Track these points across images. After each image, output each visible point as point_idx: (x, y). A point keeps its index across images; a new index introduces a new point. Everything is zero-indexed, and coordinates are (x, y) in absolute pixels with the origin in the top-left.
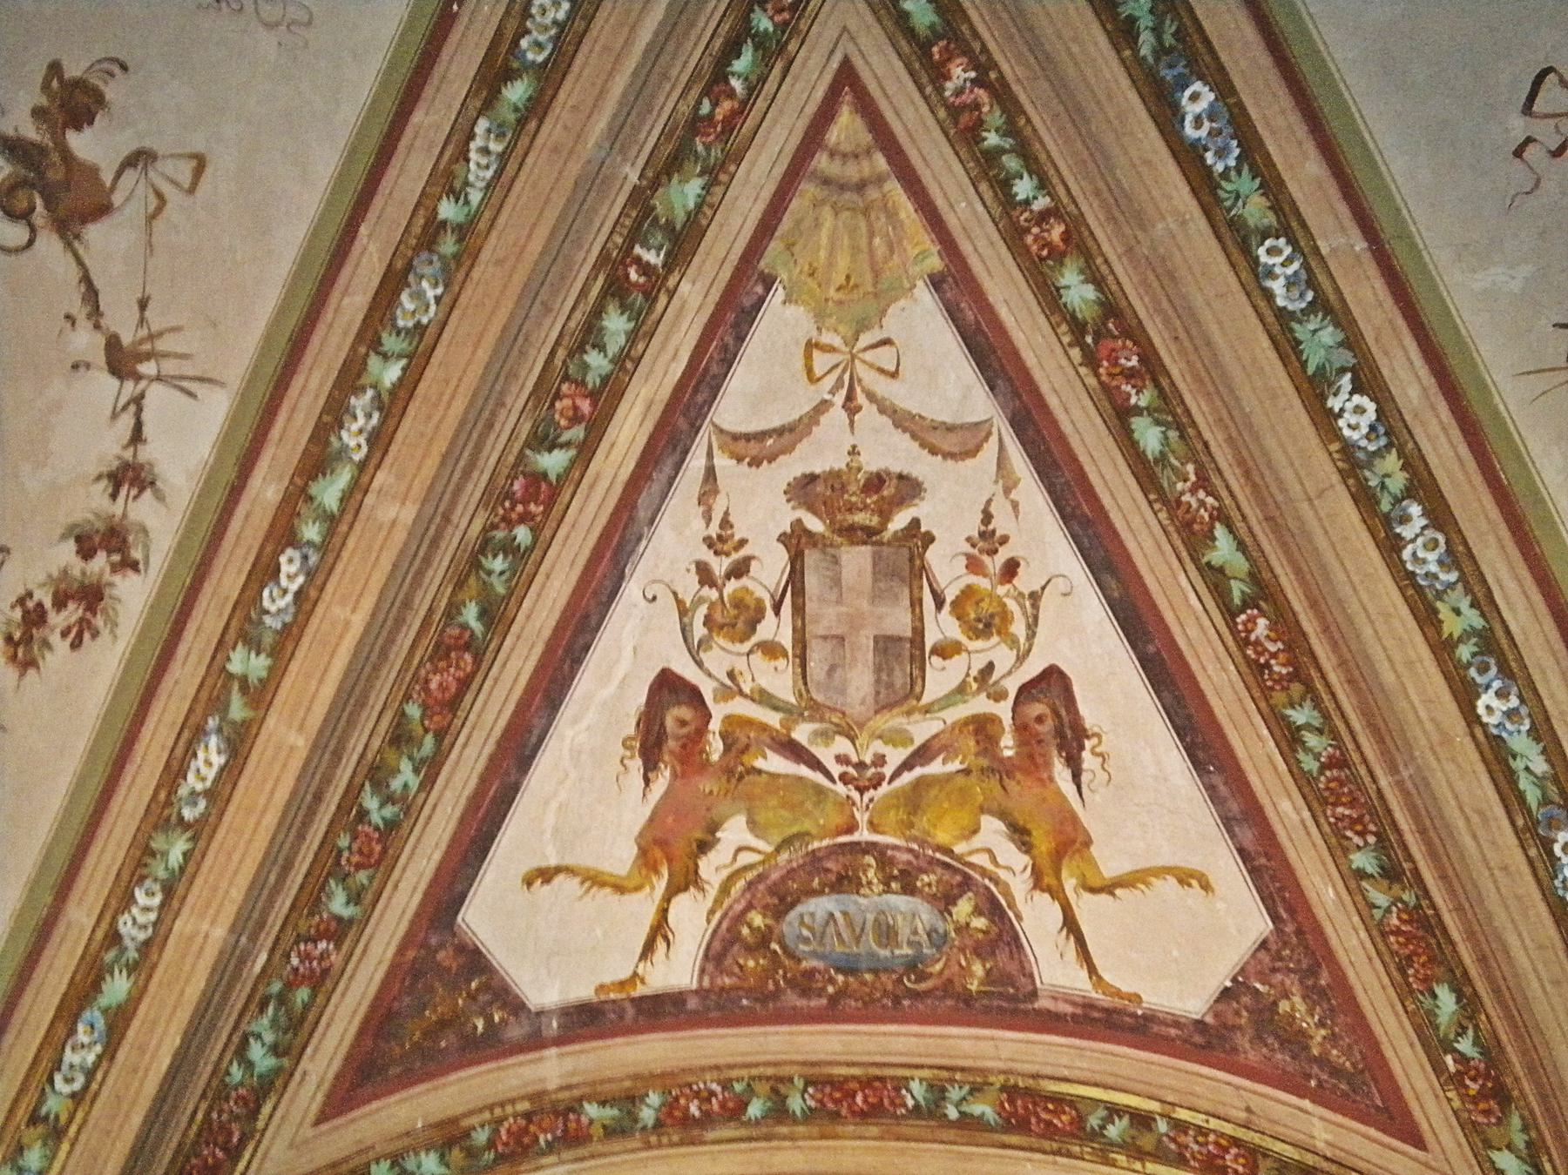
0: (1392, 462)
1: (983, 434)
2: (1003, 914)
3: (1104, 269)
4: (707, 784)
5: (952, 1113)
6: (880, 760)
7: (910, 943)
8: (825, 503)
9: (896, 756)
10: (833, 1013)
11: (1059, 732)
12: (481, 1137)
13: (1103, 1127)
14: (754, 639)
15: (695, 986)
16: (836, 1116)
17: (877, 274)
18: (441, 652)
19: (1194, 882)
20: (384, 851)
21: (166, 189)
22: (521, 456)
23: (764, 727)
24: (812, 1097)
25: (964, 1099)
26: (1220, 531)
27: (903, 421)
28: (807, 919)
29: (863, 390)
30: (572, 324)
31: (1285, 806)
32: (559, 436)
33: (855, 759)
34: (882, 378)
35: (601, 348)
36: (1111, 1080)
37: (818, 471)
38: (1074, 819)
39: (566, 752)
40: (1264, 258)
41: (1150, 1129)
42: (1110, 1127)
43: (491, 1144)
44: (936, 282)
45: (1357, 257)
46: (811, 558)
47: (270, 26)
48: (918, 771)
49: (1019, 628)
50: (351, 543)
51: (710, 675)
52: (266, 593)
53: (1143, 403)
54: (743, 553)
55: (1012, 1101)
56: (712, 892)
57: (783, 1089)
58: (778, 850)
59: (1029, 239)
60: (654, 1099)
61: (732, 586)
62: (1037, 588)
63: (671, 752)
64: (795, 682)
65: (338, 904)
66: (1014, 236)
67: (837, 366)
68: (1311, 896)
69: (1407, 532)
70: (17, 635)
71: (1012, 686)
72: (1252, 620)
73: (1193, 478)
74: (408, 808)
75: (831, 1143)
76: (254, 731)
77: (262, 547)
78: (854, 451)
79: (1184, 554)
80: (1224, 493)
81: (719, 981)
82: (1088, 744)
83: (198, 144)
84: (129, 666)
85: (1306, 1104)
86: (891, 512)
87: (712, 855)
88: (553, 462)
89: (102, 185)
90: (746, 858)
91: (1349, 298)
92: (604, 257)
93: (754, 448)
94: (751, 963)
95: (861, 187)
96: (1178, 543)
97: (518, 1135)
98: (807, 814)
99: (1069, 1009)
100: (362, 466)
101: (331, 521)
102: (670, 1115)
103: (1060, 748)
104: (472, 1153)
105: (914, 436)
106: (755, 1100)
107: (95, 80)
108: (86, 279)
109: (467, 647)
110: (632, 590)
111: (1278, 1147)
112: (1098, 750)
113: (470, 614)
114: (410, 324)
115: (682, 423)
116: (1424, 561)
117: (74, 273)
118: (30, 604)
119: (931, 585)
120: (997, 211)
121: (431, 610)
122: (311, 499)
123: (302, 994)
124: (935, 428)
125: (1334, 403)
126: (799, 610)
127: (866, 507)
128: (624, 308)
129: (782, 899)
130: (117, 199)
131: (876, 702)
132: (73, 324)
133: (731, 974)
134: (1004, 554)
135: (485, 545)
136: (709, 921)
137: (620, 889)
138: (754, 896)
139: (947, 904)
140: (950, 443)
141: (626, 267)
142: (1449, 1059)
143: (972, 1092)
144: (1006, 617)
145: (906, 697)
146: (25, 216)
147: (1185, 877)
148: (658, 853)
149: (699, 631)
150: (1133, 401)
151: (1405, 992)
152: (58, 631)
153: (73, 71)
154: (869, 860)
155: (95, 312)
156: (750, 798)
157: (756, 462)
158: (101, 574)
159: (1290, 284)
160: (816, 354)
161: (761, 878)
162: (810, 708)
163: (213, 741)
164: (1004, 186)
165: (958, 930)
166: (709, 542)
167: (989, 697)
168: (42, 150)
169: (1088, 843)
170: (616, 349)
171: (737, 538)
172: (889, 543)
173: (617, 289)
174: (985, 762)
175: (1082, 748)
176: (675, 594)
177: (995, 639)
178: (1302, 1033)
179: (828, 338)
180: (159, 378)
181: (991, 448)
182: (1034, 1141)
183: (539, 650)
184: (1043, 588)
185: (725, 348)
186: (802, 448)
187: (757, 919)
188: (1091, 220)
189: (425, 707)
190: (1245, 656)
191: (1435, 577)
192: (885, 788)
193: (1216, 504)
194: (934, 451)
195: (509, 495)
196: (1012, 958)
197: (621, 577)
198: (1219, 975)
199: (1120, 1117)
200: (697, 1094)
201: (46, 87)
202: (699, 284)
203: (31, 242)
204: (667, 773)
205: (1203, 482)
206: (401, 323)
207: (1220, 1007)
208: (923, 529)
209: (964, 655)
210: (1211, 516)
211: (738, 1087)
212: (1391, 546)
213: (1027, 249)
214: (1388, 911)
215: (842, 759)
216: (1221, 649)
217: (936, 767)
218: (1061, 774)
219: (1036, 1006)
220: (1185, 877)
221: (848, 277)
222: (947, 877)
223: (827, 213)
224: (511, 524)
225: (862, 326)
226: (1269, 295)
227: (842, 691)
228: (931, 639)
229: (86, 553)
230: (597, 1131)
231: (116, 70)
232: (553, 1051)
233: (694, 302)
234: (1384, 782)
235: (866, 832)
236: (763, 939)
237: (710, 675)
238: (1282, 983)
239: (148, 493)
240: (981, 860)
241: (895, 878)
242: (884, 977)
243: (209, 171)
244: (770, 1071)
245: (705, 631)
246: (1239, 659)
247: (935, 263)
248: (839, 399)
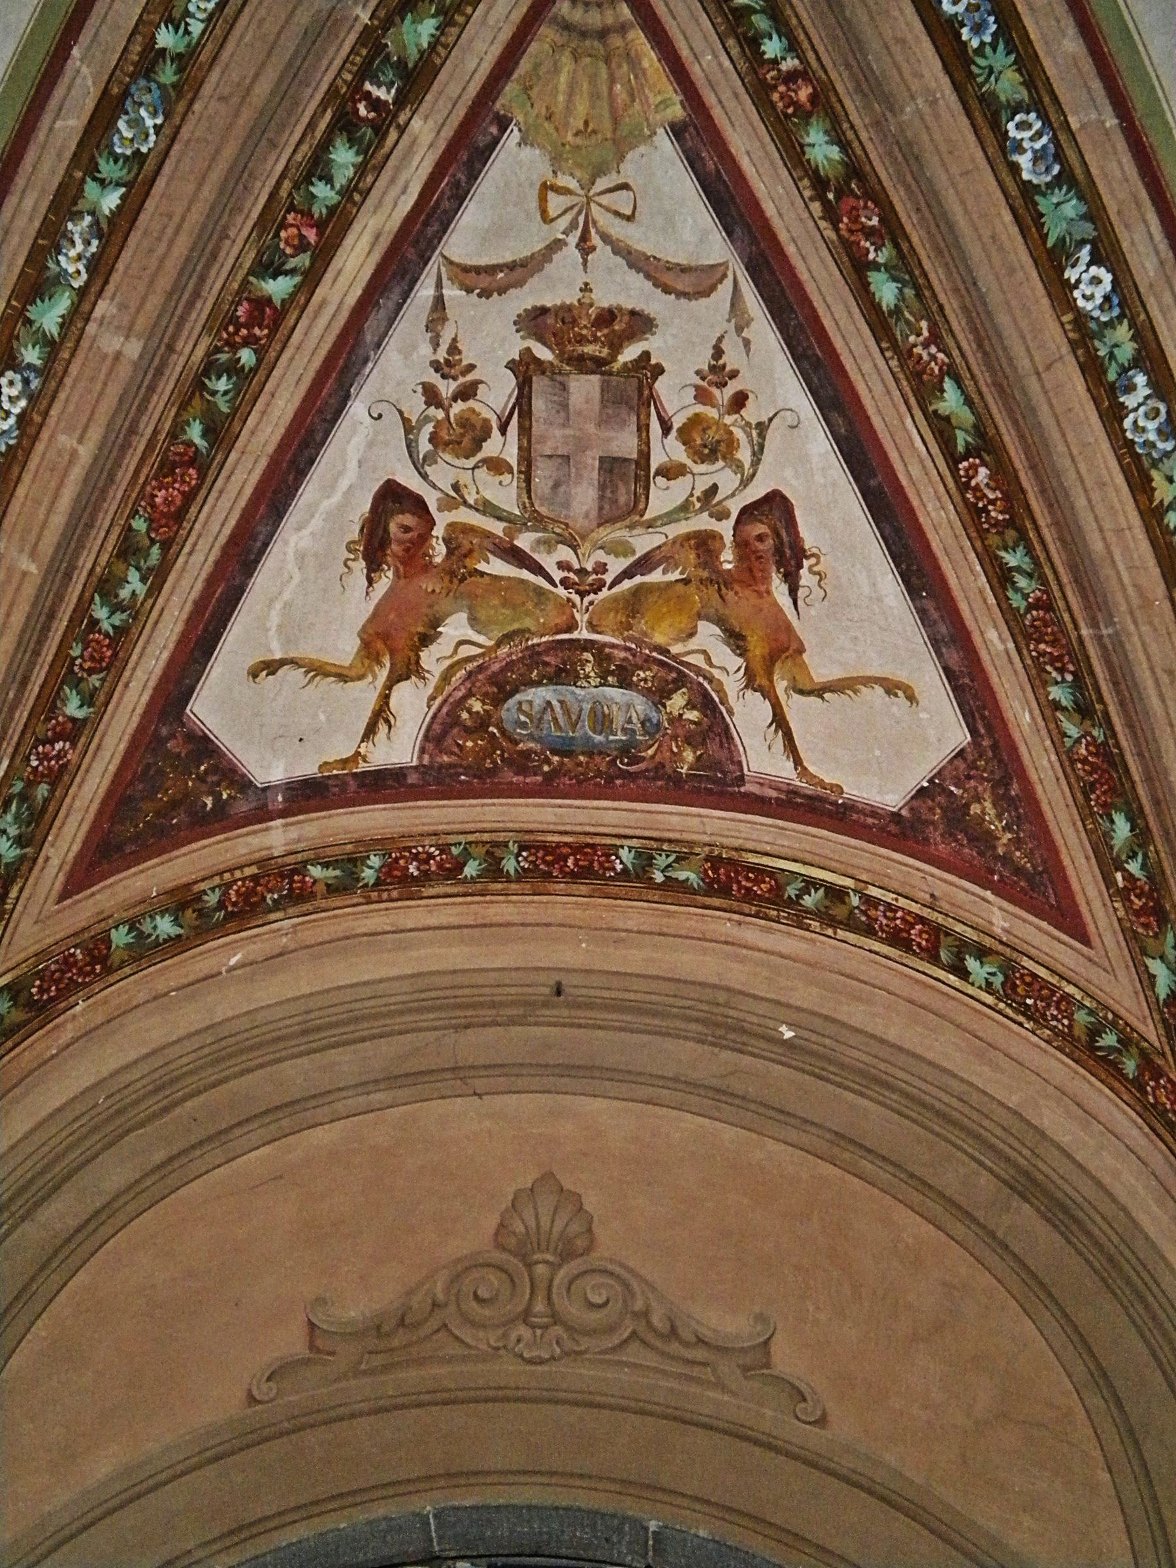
0: (1123, 332)
1: (719, 275)
2: (715, 708)
3: (850, 135)
4: (428, 584)
5: (659, 877)
6: (602, 568)
7: (624, 730)
8: (554, 335)
9: (616, 566)
10: (548, 789)
11: (779, 551)
12: (212, 899)
13: (799, 897)
14: (480, 456)
15: (415, 763)
16: (547, 876)
17: (616, 121)
18: (167, 469)
19: (900, 693)
20: (115, 655)
22: (245, 283)
23: (488, 535)
24: (525, 859)
25: (669, 866)
26: (948, 384)
27: (637, 262)
28: (525, 707)
29: (598, 232)
30: (299, 157)
31: (992, 635)
32: (284, 264)
33: (576, 566)
34: (617, 221)
35: (329, 180)
36: (809, 857)
37: (549, 305)
38: (789, 628)
39: (291, 556)
40: (1013, 132)
41: (844, 903)
42: (806, 897)
43: (221, 905)
44: (677, 131)
45: (1107, 133)
46: (539, 383)
48: (638, 579)
49: (744, 455)
50: (74, 370)
51: (434, 486)
53: (881, 259)
54: (469, 377)
55: (715, 869)
56: (433, 681)
57: (498, 852)
58: (498, 644)
59: (775, 97)
60: (375, 861)
61: (458, 408)
62: (765, 419)
63: (395, 555)
64: (519, 496)
65: (73, 708)
66: (760, 93)
67: (571, 208)
68: (1009, 715)
69: (1130, 401)
71: (735, 509)
72: (974, 467)
73: (926, 333)
74: (135, 612)
75: (544, 898)
78: (586, 288)
79: (912, 401)
80: (955, 353)
81: (439, 759)
82: (806, 563)
85: (988, 894)
86: (621, 346)
87: (433, 647)
88: (278, 288)
90: (466, 651)
91: (1094, 171)
92: (333, 91)
93: (485, 281)
94: (470, 744)
95: (603, 34)
96: (907, 389)
97: (246, 896)
98: (527, 613)
99: (774, 794)
100: (82, 292)
101: (52, 346)
102: (389, 874)
103: (779, 564)
104: (201, 913)
105: (648, 276)
106: (471, 862)
109: (191, 463)
110: (357, 409)
111: (959, 928)
112: (815, 569)
113: (195, 432)
114: (129, 152)
115: (411, 254)
116: (1144, 430)
119: (658, 413)
120: (743, 66)
121: (156, 432)
122: (30, 322)
123: (42, 790)
124: (668, 269)
125: (1071, 275)
126: (525, 431)
127: (596, 340)
128: (352, 142)
129: (501, 688)
131: (600, 516)
133: (452, 753)
134: (732, 388)
135: (210, 368)
136: (429, 707)
137: (343, 677)
138: (473, 684)
139: (662, 697)
140: (683, 283)
141: (355, 102)
142: (1119, 876)
143: (677, 860)
144: (731, 444)
145: (629, 514)
147: (891, 687)
148: (380, 645)
149: (424, 446)
150: (871, 256)
151: (1086, 813)
154: (587, 656)
156: (472, 596)
157: (486, 294)
159: (1038, 157)
160: (551, 195)
161: (480, 668)
162: (537, 521)
164: (752, 43)
165: (671, 721)
166: (436, 366)
167: (711, 516)
169: (801, 650)
170: (344, 182)
171: (465, 363)
172: (618, 374)
173: (345, 124)
174: (705, 574)
175: (801, 567)
176: (401, 413)
177: (721, 463)
178: (989, 833)
179: (564, 181)
181: (726, 288)
182: (735, 905)
183: (263, 463)
184: (771, 420)
185: (456, 185)
186: (534, 282)
187: (477, 706)
188: (840, 88)
189: (150, 520)
190: (965, 500)
191: (1153, 445)
192: (605, 593)
193: (946, 360)
194: (667, 290)
195: (233, 320)
196: (721, 746)
197: (347, 397)
198: (918, 775)
199: (816, 890)
200: (416, 857)
202: (431, 122)
204: (390, 574)
205: (935, 338)
207: (915, 803)
208: (653, 361)
209: (689, 476)
210: (941, 369)
211: (455, 851)
212: (1113, 415)
213: (773, 105)
214: (1078, 741)
215: (563, 566)
216: (942, 489)
217: (656, 577)
218: (779, 590)
219: (742, 789)
220: (891, 687)
221: (586, 123)
222: (662, 673)
223: (566, 59)
224: (234, 347)
225: (599, 171)
226: (1015, 169)
227: (567, 505)
228: (657, 460)
230: (320, 888)
232: (279, 822)
233: (426, 138)
234: (1085, 632)
235: (585, 631)
236: (481, 724)
237: (434, 486)
238: (976, 788)
240: (697, 660)
241: (612, 673)
242: (598, 759)
244: (486, 837)
245: (430, 447)
246: (957, 498)
247: (677, 112)
248: (573, 239)
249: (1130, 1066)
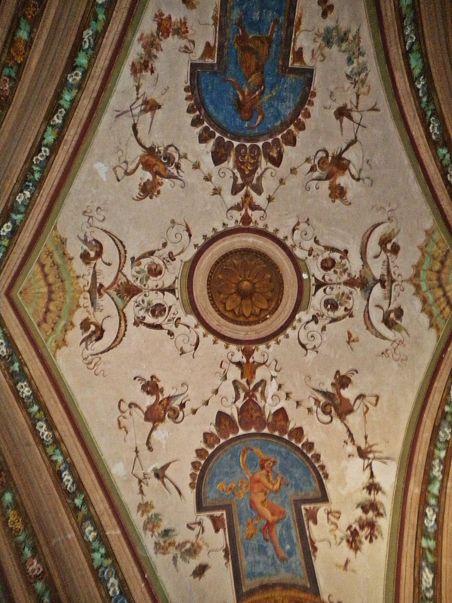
21: (369, 405)
47: (396, 360)
52: (425, 521)
70: (351, 540)
76: (440, 566)
77: (419, 508)
83: (376, 392)
84: (390, 547)
89: (350, 405)
100: (442, 481)
101: (438, 498)
107: (349, 376)
108: (349, 430)
114: (444, 441)
117: (345, 429)
118: (352, 529)
130: (355, 408)
132: (347, 443)
146: (329, 413)
152: (364, 538)
153: (343, 373)
155: (353, 440)
158: (372, 518)
163: (427, 570)
168: (333, 395)
180: (374, 458)
201: (335, 377)
203: (331, 421)
206: (441, 441)
229: (366, 511)
231: (355, 373)
239: (380, 492)
243: (380, 400)
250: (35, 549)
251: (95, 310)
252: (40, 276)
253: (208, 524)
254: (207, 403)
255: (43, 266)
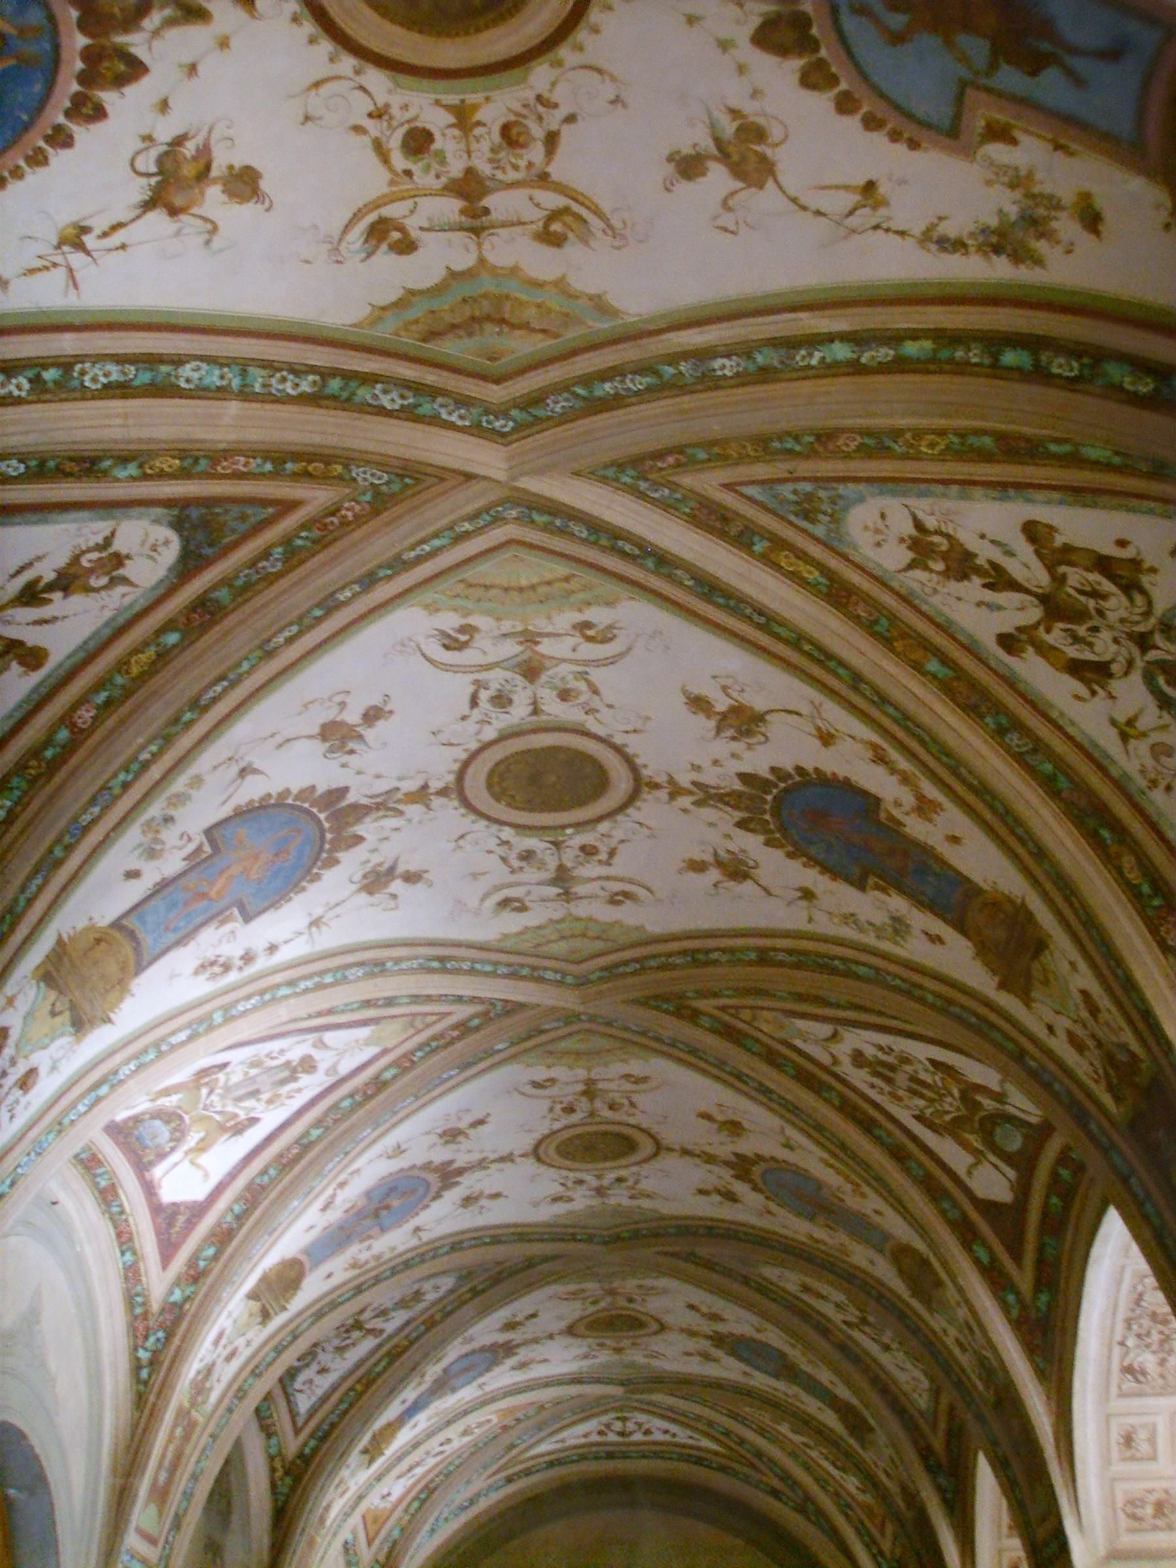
234: (266, 1203)
249: (138, 1311)
250: (108, 703)
251: (494, 638)
252: (548, 576)
253: (191, 847)
254: (359, 773)
255: (567, 579)
